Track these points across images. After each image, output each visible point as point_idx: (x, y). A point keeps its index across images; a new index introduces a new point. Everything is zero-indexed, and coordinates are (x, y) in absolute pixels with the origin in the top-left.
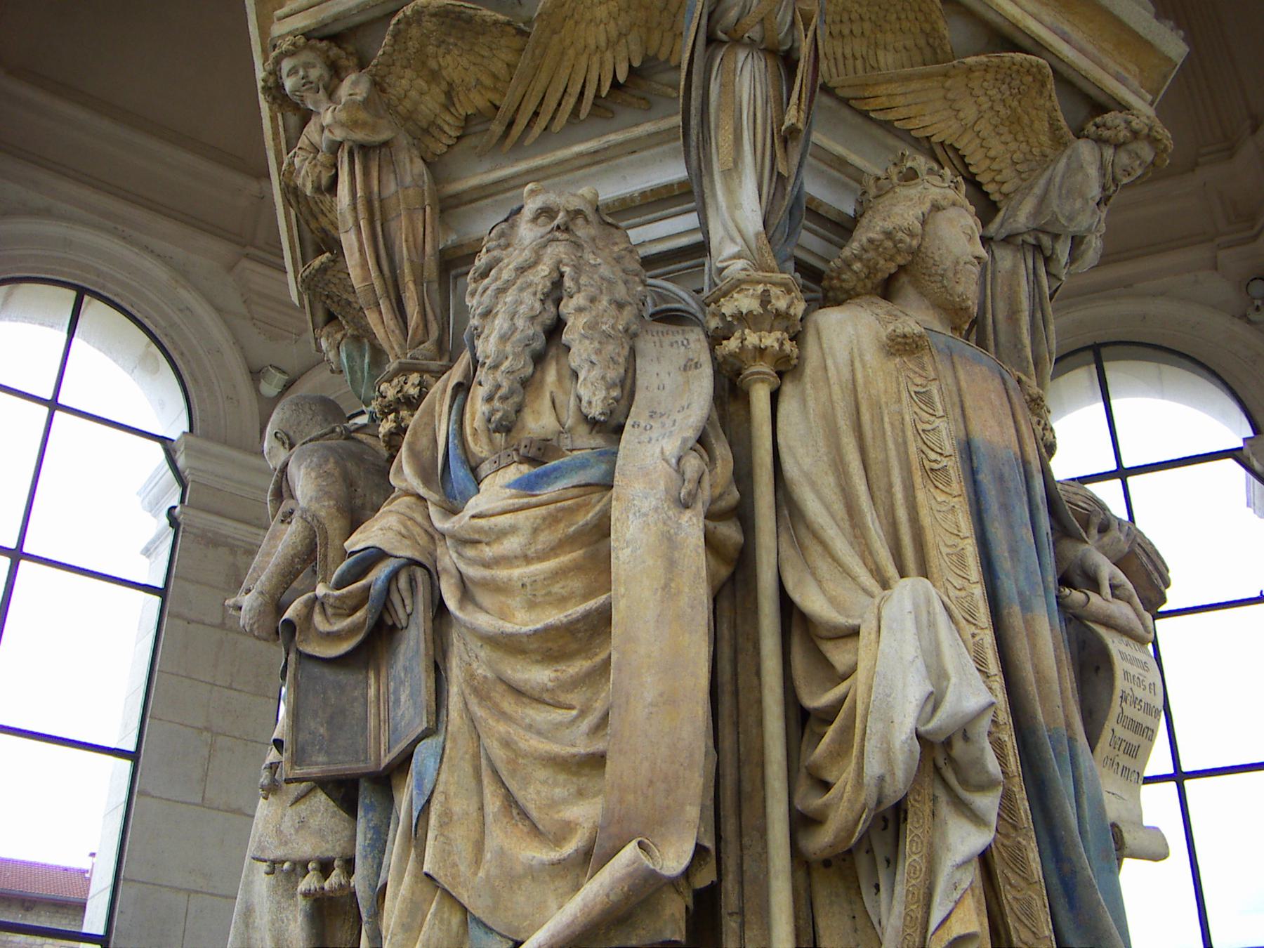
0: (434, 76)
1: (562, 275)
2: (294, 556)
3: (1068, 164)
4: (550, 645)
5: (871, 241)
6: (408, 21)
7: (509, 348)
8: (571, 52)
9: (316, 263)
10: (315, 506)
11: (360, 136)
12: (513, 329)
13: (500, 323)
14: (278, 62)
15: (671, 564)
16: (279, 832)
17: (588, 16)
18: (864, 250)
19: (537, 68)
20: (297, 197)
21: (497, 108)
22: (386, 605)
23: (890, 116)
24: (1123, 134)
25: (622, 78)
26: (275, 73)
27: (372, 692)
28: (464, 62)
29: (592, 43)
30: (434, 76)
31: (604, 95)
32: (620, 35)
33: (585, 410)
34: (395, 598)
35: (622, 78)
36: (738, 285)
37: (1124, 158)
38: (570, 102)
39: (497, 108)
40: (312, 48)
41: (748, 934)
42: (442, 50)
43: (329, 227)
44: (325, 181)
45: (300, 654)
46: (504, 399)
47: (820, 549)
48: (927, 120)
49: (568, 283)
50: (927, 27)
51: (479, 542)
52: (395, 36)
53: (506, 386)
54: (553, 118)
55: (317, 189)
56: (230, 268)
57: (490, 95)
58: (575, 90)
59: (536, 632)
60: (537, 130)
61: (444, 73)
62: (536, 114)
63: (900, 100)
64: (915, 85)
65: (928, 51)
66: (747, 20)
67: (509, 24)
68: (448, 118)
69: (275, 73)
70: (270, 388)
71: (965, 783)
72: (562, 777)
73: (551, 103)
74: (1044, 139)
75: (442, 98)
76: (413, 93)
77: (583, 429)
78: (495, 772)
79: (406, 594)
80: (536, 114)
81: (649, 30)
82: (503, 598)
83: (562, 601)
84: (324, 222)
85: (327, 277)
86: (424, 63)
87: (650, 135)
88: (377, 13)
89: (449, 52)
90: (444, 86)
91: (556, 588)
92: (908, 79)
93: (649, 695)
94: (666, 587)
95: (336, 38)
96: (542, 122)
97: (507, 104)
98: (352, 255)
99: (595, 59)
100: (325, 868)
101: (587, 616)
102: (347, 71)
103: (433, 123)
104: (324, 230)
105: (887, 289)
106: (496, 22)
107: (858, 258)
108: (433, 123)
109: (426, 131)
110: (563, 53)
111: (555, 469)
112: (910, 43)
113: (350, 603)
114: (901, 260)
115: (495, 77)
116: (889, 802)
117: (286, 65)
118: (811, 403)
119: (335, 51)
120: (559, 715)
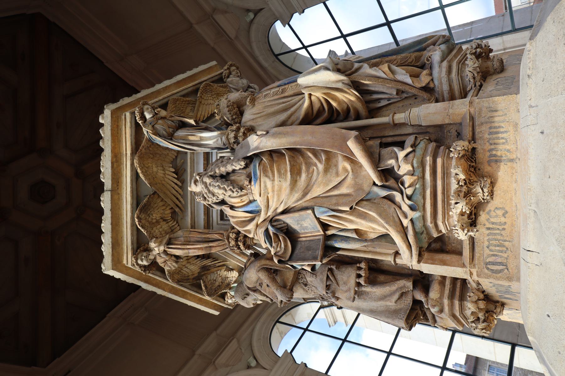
0: (158, 222)
1: (211, 176)
2: (268, 276)
3: (231, 84)
4: (296, 172)
5: (228, 111)
6: (140, 221)
7: (222, 187)
8: (163, 182)
9: (203, 288)
10: (256, 268)
11: (165, 241)
12: (218, 186)
13: (216, 190)
14: (138, 264)
15: (280, 133)
16: (346, 291)
17: (155, 173)
18: (230, 114)
19: (165, 193)
20: (180, 282)
21: (172, 208)
22: (280, 229)
23: (206, 117)
24: (228, 71)
25: (174, 170)
26: (141, 266)
27: (304, 239)
28: (156, 211)
29: (162, 175)
30: (158, 222)
31: (176, 177)
32: (162, 167)
33: (242, 167)
34: (279, 226)
35: (174, 170)
36: (228, 139)
37: (233, 73)
38: (176, 187)
39: (172, 208)
40: (138, 254)
41: (387, 135)
42: (151, 216)
43: (193, 277)
44: (174, 259)
45: (288, 260)
46: (234, 188)
47: (293, 117)
48: (210, 110)
49: (212, 173)
50: (187, 102)
51: (268, 197)
52: (143, 228)
53: (231, 187)
54: (180, 194)
55: (176, 262)
56: (216, 369)
57: (168, 208)
58: (174, 185)
59: (291, 174)
60: (181, 199)
61: (158, 218)
62: (177, 198)
63: (203, 114)
64: (200, 109)
65: (193, 105)
66: (167, 130)
67: (150, 196)
68: (170, 223)
69: (141, 266)
70: (253, 363)
71: (351, 69)
72: (331, 170)
73: (175, 192)
74: (224, 90)
75: (165, 223)
76: (161, 230)
77: (247, 169)
78: (327, 192)
79: (278, 223)
80: (177, 198)
81: (164, 161)
82: (283, 190)
83: (286, 171)
84: (191, 277)
85: (209, 287)
86: (153, 223)
87: (191, 168)
88: (135, 233)
89: (152, 215)
90: (161, 220)
91: (282, 172)
92: (198, 110)
93: (310, 138)
94: (285, 134)
95: (138, 248)
96: (179, 197)
97: (172, 205)
98: (195, 252)
99: (167, 176)
100: (359, 276)
101: (289, 161)
102: (147, 247)
103: (170, 228)
104: (194, 279)
105: (242, 113)
106: (148, 198)
107: (232, 116)
108: (170, 228)
109: (172, 231)
110: (163, 184)
111: (254, 173)
112: (190, 108)
113: (277, 240)
114: (235, 106)
115: (164, 205)
116: (351, 84)
117: (140, 262)
118: (260, 123)
119: (141, 249)
120: (315, 173)
